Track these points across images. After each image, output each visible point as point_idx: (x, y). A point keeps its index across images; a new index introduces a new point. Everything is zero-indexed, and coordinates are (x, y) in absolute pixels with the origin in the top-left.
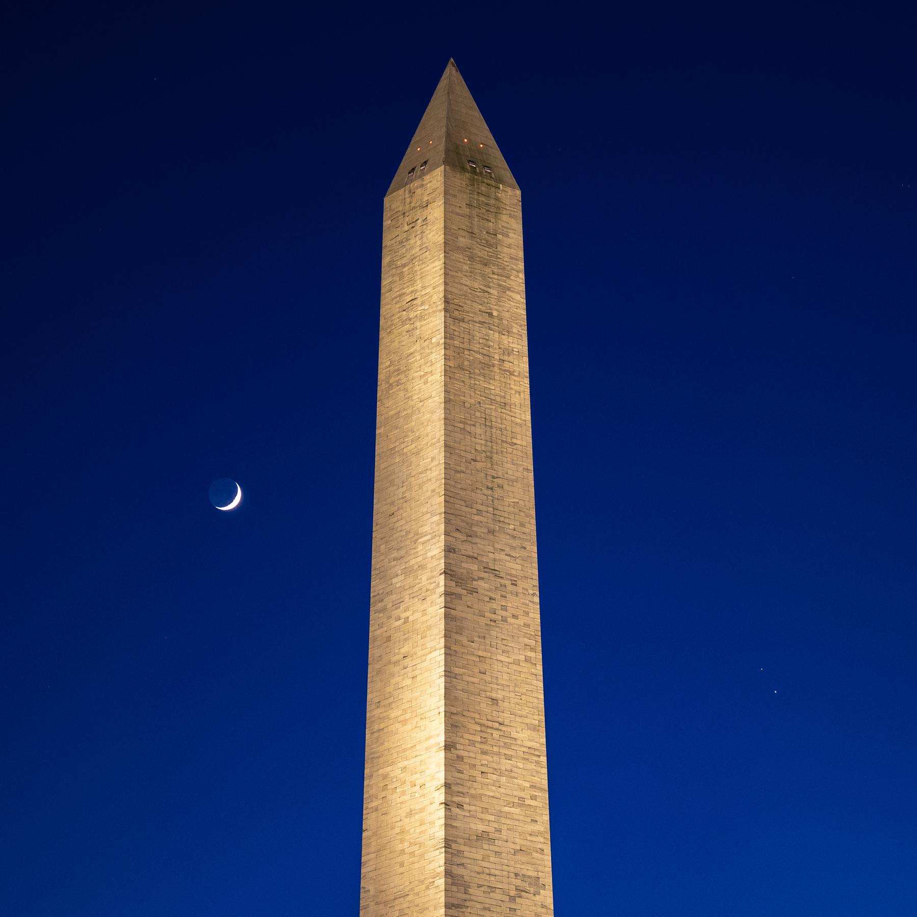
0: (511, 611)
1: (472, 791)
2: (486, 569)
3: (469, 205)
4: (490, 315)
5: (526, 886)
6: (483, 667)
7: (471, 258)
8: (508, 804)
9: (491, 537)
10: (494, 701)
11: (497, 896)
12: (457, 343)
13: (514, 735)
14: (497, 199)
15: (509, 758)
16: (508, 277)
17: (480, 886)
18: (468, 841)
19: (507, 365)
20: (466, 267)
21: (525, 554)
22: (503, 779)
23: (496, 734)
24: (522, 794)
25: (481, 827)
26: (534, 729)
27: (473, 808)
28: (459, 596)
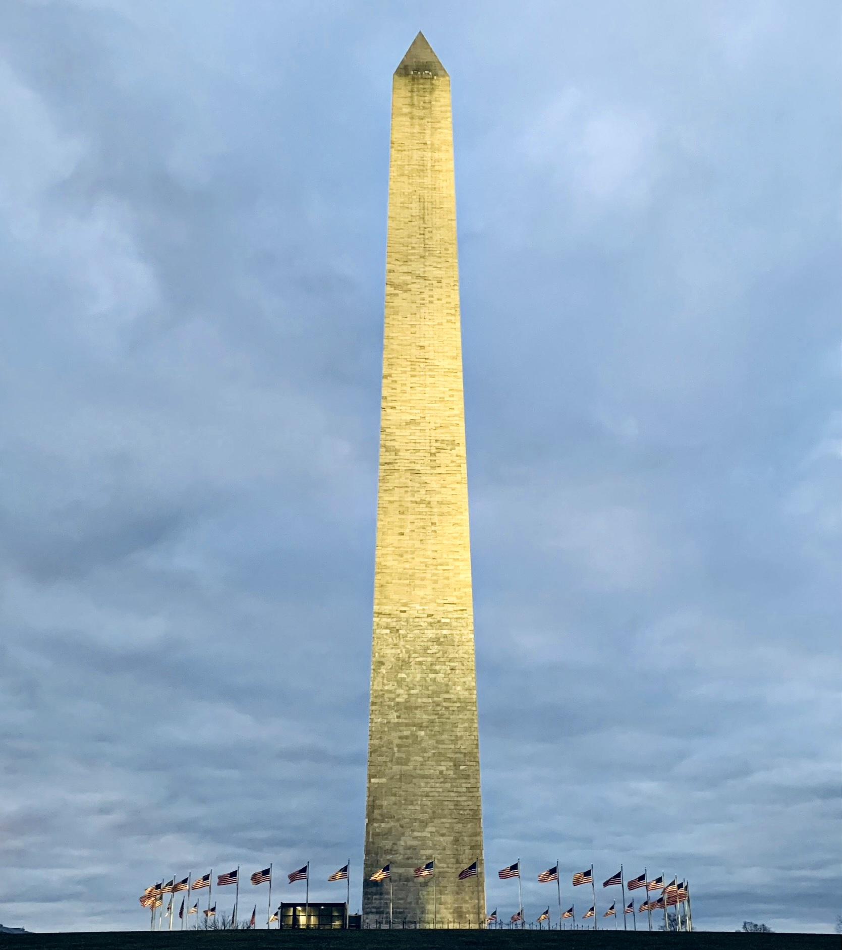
0: (436, 297)
1: (404, 398)
2: (418, 277)
3: (412, 91)
4: (425, 144)
5: (444, 446)
6: (413, 330)
7: (412, 118)
8: (431, 402)
9: (422, 260)
10: (422, 347)
11: (422, 454)
12: (399, 163)
13: (436, 363)
14: (432, 84)
15: (433, 377)
16: (439, 122)
17: (407, 450)
18: (399, 426)
19: (437, 168)
20: (407, 123)
21: (447, 264)
22: (428, 389)
23: (422, 365)
24: (442, 395)
25: (408, 418)
26: (455, 358)
27: (402, 408)
28: (397, 295)
